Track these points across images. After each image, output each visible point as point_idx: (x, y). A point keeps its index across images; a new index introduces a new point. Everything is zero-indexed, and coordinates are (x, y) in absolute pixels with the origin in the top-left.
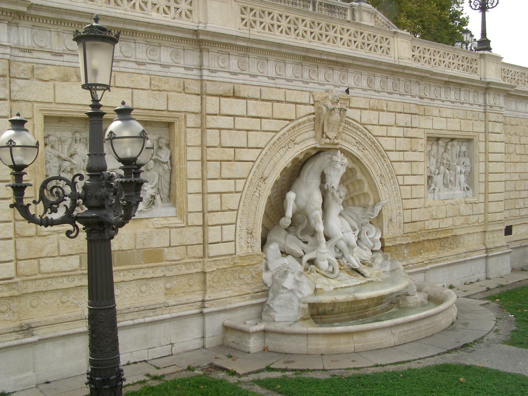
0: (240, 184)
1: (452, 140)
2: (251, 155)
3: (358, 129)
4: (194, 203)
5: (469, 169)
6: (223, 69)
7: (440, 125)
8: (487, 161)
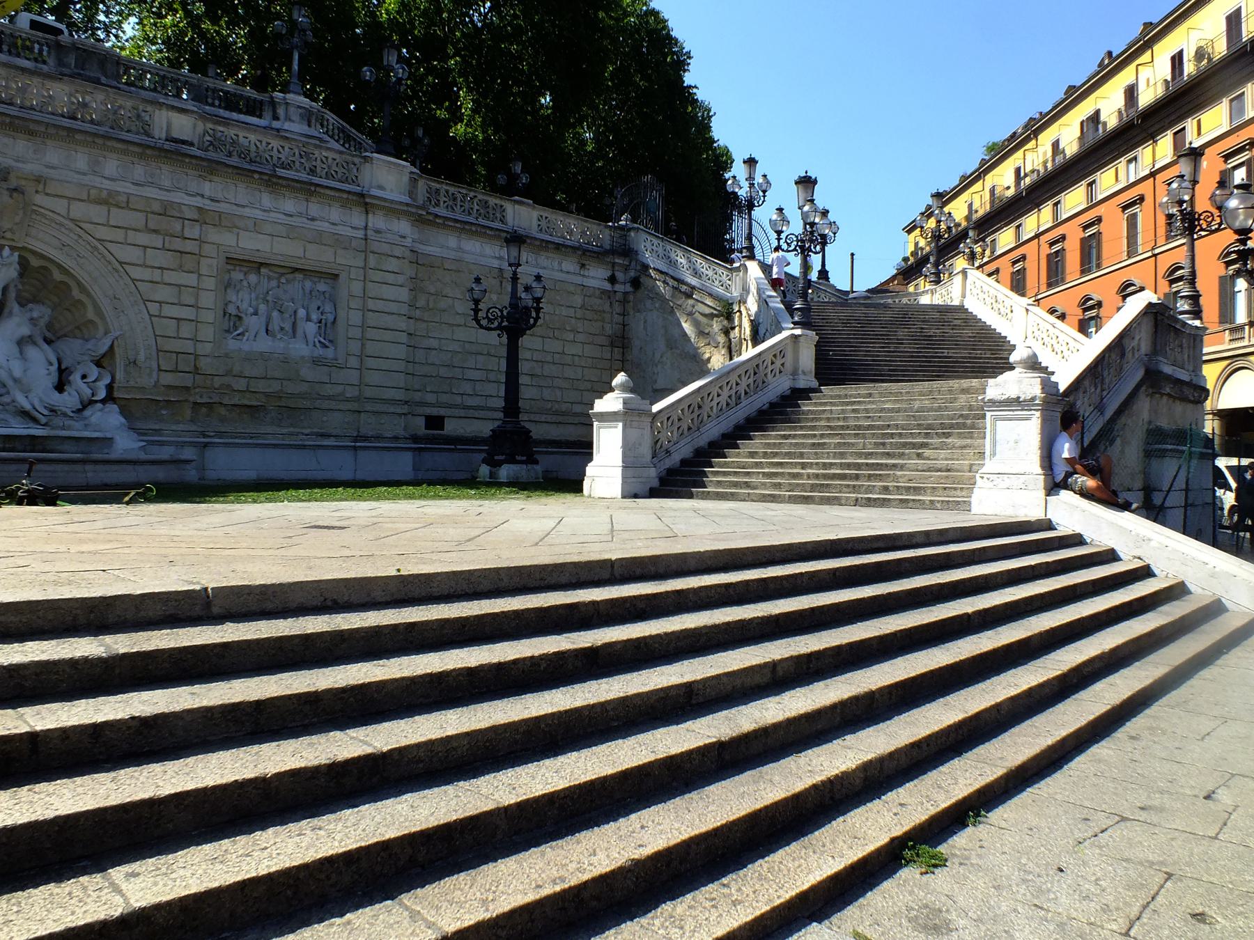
1: (296, 270)
3: (61, 225)
5: (331, 318)
7: (250, 244)
8: (365, 310)
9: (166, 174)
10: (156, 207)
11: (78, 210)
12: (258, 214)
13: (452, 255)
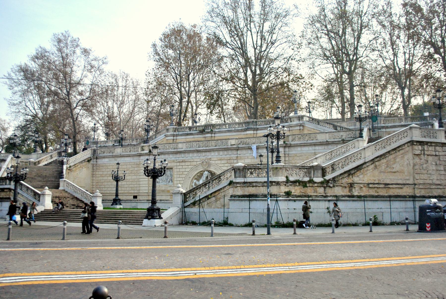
0: (183, 179)
2: (186, 173)
4: (175, 182)
6: (180, 157)
9: (230, 152)
10: (229, 158)
11: (217, 162)
12: (248, 155)
13: (299, 152)
